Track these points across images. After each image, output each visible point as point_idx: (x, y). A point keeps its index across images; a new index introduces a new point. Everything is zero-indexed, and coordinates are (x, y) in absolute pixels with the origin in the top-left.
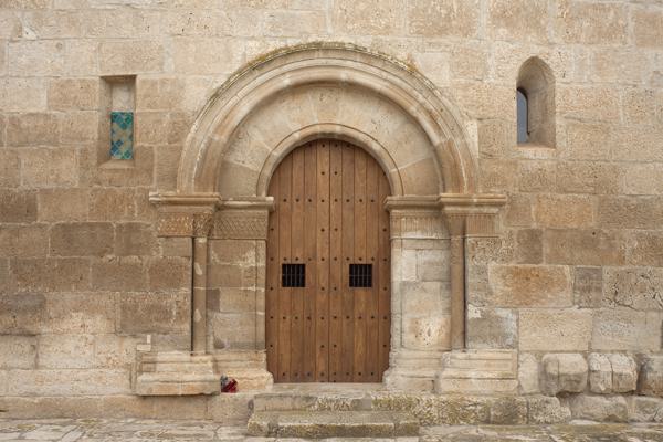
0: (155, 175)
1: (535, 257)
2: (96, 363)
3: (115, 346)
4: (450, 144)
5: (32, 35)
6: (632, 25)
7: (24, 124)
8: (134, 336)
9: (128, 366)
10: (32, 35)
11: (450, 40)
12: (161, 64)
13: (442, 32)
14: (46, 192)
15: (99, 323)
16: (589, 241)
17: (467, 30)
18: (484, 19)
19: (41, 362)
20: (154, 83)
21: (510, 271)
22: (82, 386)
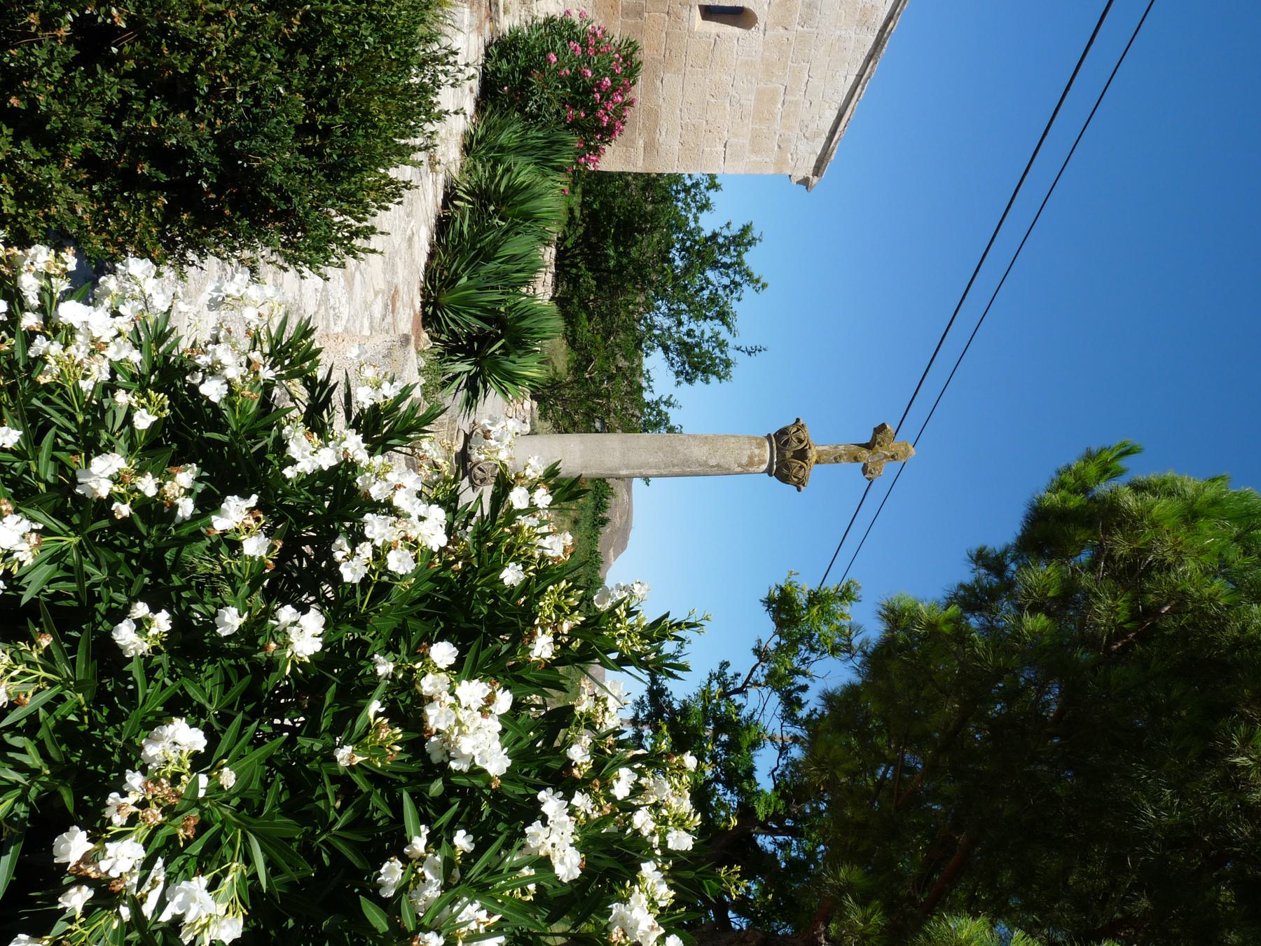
6: (770, 86)
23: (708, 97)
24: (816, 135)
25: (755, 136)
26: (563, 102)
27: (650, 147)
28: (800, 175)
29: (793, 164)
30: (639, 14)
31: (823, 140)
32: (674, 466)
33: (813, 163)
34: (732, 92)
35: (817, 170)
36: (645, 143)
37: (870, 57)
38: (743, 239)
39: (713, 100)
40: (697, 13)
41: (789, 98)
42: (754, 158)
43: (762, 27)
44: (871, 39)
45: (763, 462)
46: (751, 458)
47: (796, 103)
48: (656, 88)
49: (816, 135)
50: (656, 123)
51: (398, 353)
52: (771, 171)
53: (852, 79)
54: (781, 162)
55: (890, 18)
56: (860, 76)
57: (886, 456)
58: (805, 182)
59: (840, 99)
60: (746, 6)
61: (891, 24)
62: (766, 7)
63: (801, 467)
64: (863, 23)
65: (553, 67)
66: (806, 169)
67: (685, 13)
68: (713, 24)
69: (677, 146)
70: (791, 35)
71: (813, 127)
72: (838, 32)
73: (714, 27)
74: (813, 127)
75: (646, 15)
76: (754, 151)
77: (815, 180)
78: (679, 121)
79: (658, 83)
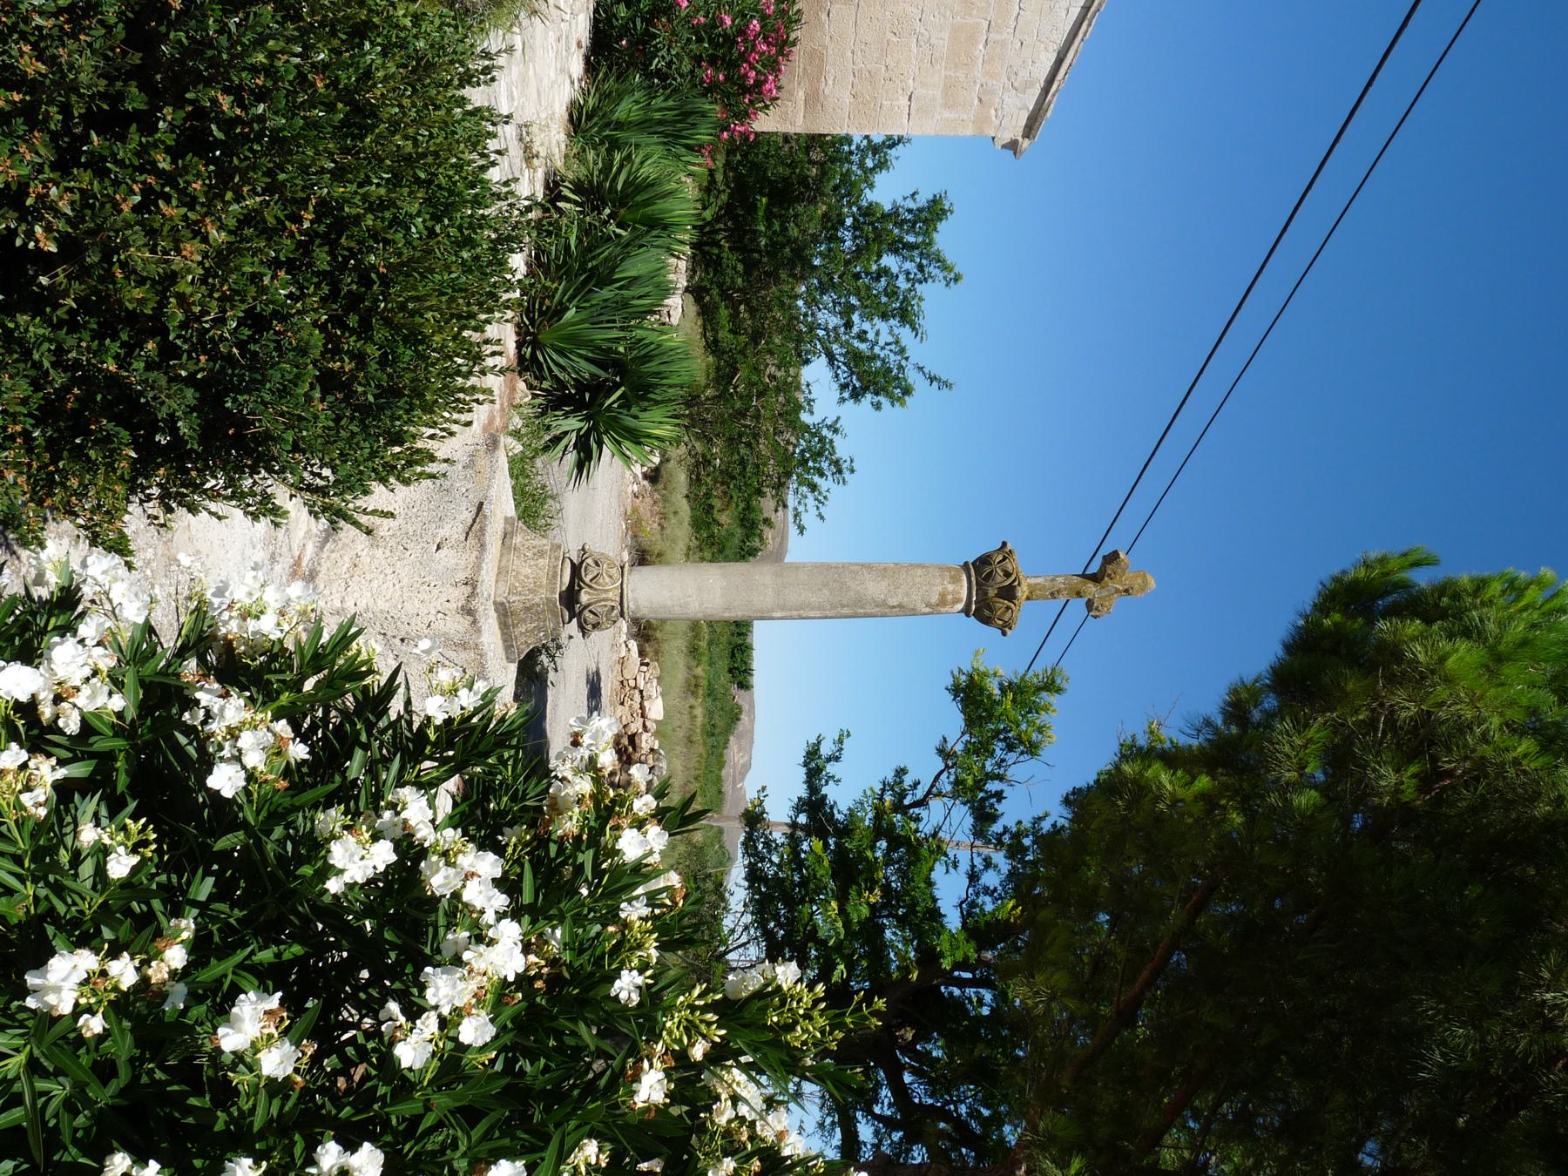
6: (970, 21)
23: (889, 35)
24: (1028, 85)
25: (949, 87)
26: (697, 60)
27: (813, 100)
28: (1006, 137)
29: (997, 122)
31: (1038, 92)
32: (843, 606)
33: (1023, 122)
35: (1030, 130)
36: (807, 95)
38: (934, 212)
39: (895, 39)
41: (992, 36)
42: (947, 114)
45: (958, 601)
46: (943, 596)
47: (1003, 44)
48: (821, 24)
49: (1028, 85)
50: (821, 69)
51: (482, 462)
52: (969, 132)
53: (1075, 12)
54: (982, 120)
57: (1117, 591)
58: (1013, 146)
59: (1060, 38)
63: (1008, 608)
65: (683, 14)
66: (1013, 129)
69: (847, 99)
71: (1023, 74)
74: (1023, 74)
76: (946, 106)
77: (1026, 143)
78: (850, 66)
79: (824, 16)
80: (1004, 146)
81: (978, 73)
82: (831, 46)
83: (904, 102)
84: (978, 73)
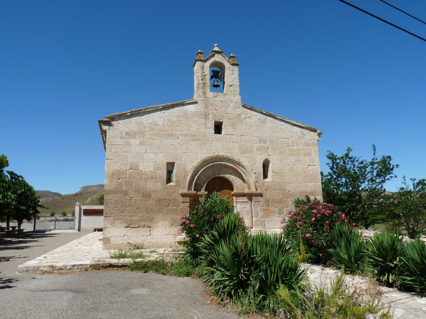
0: (181, 187)
1: (268, 206)
2: (166, 234)
3: (171, 229)
4: (248, 179)
5: (149, 152)
6: (287, 151)
7: (148, 174)
8: (176, 227)
9: (174, 235)
10: (149, 152)
11: (248, 155)
12: (181, 159)
13: (246, 153)
14: (154, 191)
15: (167, 223)
16: (280, 201)
17: (251, 152)
18: (255, 149)
19: (152, 234)
20: (180, 164)
21: (264, 209)
22: (163, 240)
23: (293, 173)
24: (302, 133)
25: (305, 155)
26: (324, 232)
28: (317, 137)
30: (268, 201)
31: (304, 130)
34: (291, 165)
35: (314, 131)
37: (275, 118)
39: (294, 172)
40: (265, 180)
42: (313, 155)
43: (269, 157)
44: (269, 118)
47: (293, 141)
48: (292, 193)
49: (302, 133)
53: (283, 123)
54: (313, 145)
55: (262, 113)
56: (281, 120)
58: (319, 135)
60: (262, 163)
61: (264, 112)
62: (262, 156)
64: (264, 122)
65: (311, 235)
66: (314, 135)
67: (266, 184)
68: (269, 174)
69: (312, 184)
70: (270, 146)
71: (300, 135)
72: (268, 130)
73: (270, 174)
74: (300, 135)
75: (268, 198)
76: (311, 155)
77: (318, 131)
78: (303, 184)
79: (290, 192)
80: (320, 137)
81: (301, 147)
82: (298, 190)
83: (311, 167)
84: (301, 147)
